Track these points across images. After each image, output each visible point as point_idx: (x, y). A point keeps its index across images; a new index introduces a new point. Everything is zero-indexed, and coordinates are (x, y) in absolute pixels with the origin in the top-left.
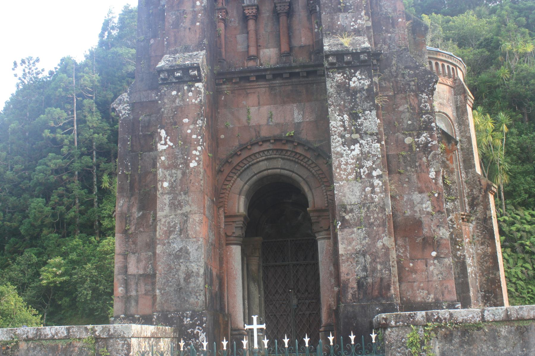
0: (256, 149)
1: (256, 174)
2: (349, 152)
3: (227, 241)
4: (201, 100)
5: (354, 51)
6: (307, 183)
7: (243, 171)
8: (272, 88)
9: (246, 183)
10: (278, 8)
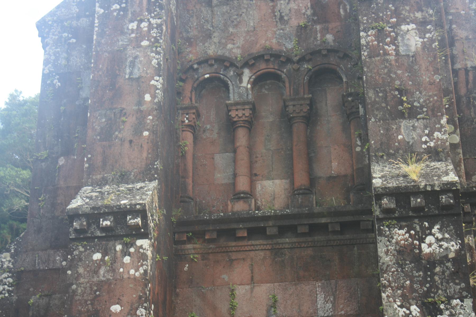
4: (146, 271)
5: (429, 189)
8: (276, 252)
10: (290, 109)
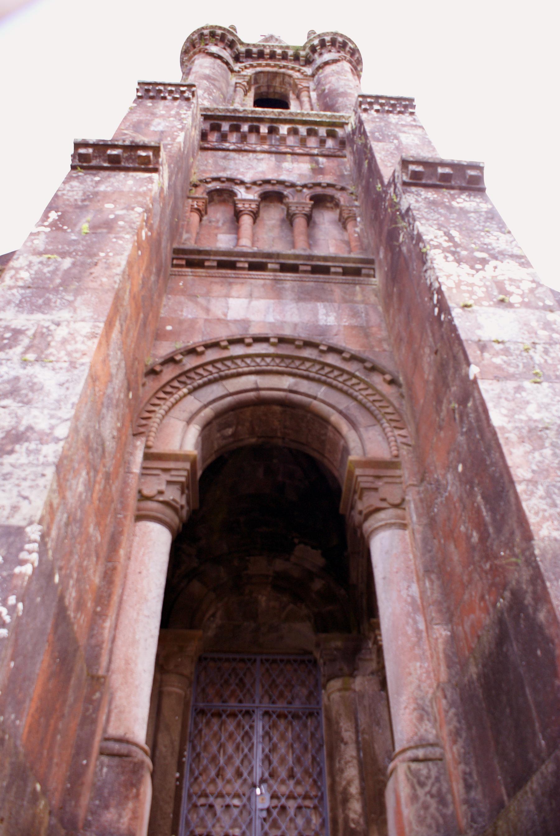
0: (237, 350)
2: (474, 272)
3: (139, 509)
9: (206, 406)
10: (293, 208)
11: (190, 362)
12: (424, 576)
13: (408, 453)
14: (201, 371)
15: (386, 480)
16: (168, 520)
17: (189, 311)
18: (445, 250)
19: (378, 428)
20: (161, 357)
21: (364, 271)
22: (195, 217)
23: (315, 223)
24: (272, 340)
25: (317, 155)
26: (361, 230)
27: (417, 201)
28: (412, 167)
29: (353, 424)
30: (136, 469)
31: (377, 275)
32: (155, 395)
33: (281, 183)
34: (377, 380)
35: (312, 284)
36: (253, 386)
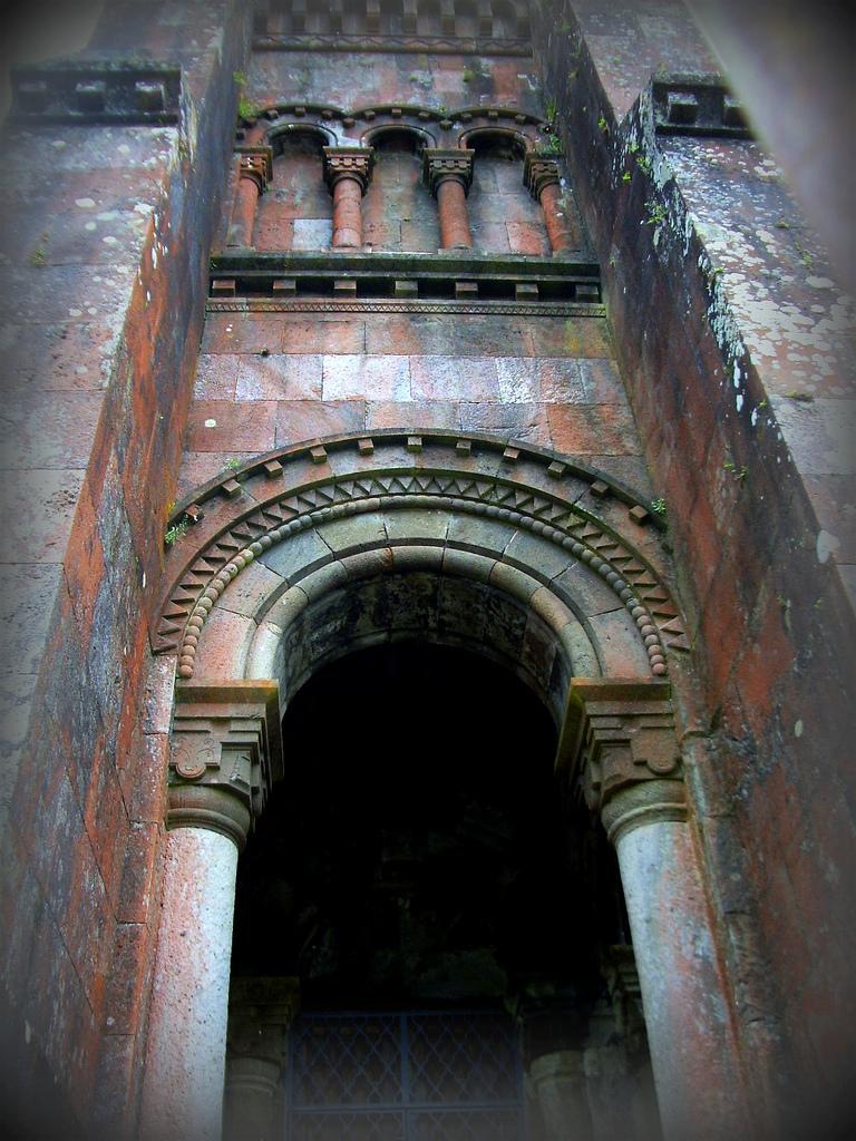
0: (347, 465)
1: (336, 556)
3: (172, 805)
6: (560, 594)
7: (285, 538)
9: (289, 583)
10: (437, 164)
11: (255, 495)
12: (724, 919)
13: (684, 668)
14: (277, 512)
15: (643, 722)
16: (229, 821)
17: (248, 387)
18: (752, 274)
19: (622, 613)
20: (200, 487)
21: (579, 291)
22: (250, 189)
23: (478, 189)
24: (411, 442)
25: (477, 53)
26: (570, 203)
27: (687, 168)
28: (674, 98)
29: (578, 613)
30: (163, 725)
31: (605, 296)
32: (190, 568)
33: (412, 112)
34: (616, 517)
35: (481, 319)
36: (381, 537)
